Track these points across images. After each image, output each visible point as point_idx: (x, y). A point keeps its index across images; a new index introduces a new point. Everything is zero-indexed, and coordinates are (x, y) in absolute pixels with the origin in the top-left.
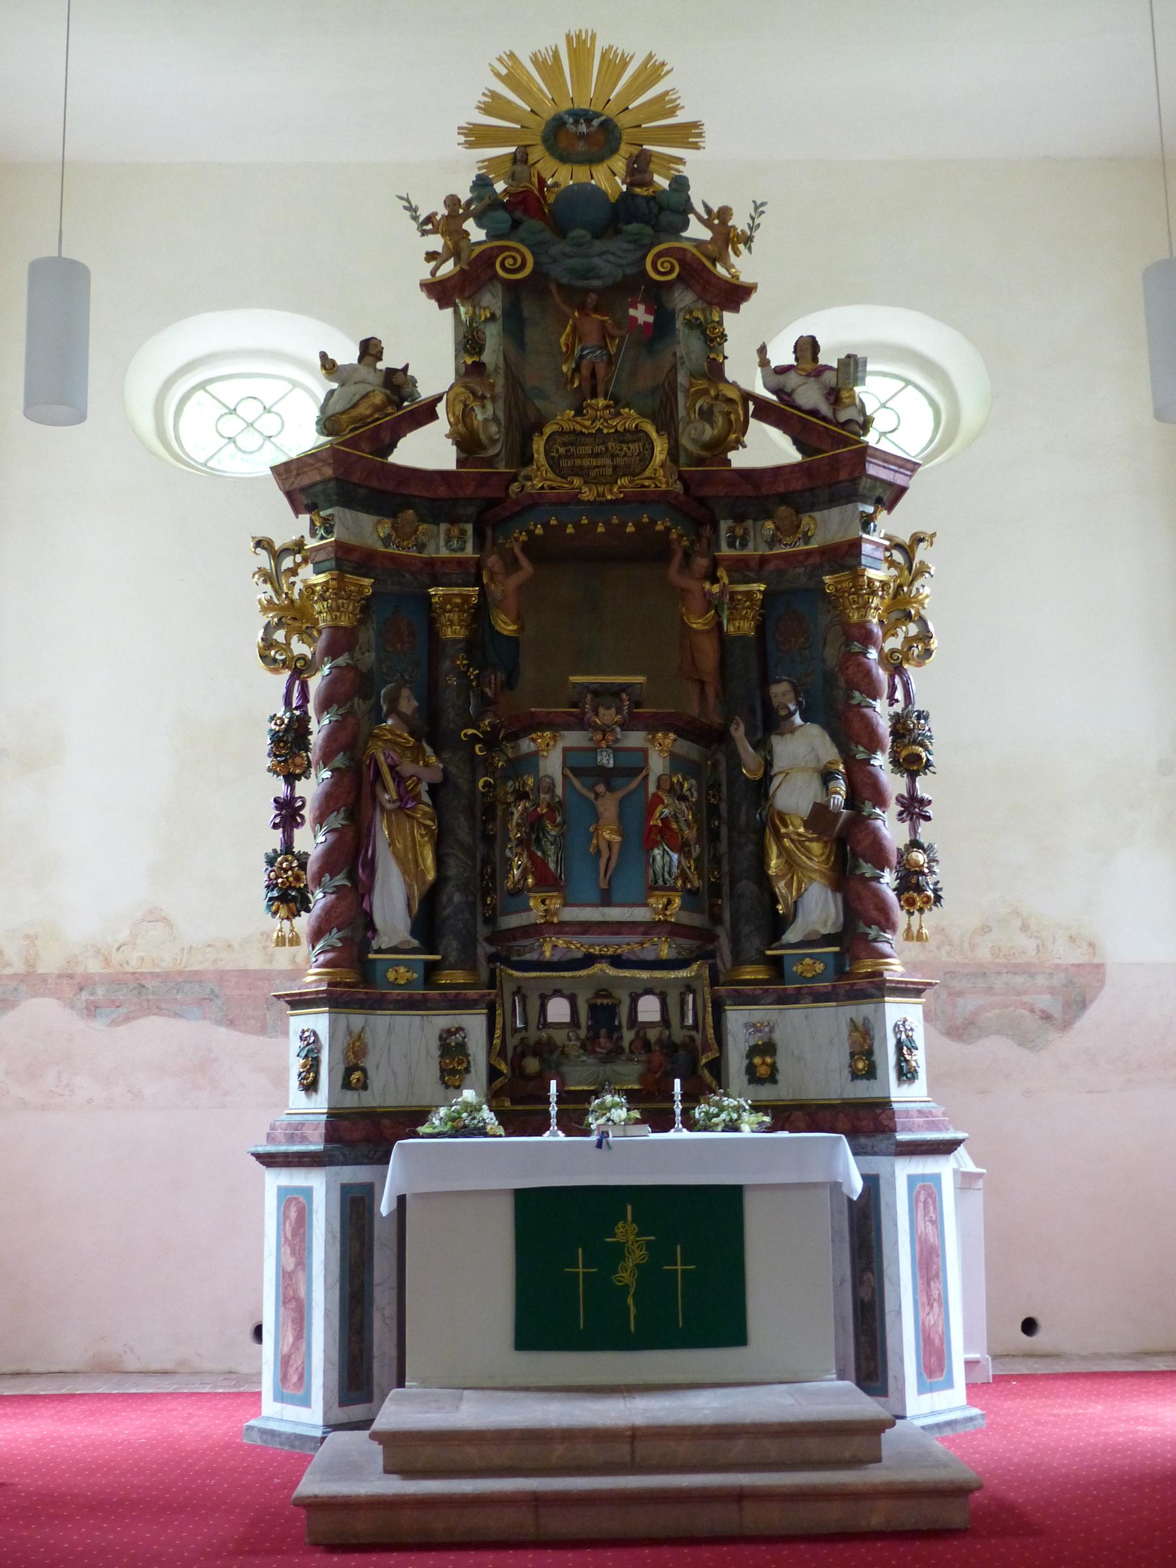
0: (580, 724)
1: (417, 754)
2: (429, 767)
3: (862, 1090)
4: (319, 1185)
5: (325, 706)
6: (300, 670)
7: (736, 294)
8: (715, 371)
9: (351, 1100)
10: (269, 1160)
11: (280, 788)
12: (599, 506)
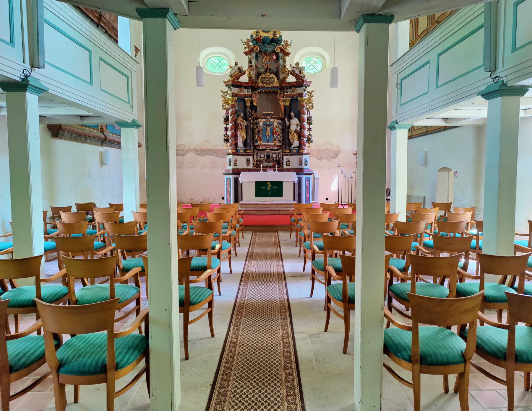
0: (265, 118)
1: (243, 121)
2: (245, 123)
3: (300, 167)
4: (232, 177)
5: (231, 115)
7: (288, 54)
8: (285, 67)
9: (235, 167)
10: (225, 174)
11: (225, 126)
12: (268, 88)
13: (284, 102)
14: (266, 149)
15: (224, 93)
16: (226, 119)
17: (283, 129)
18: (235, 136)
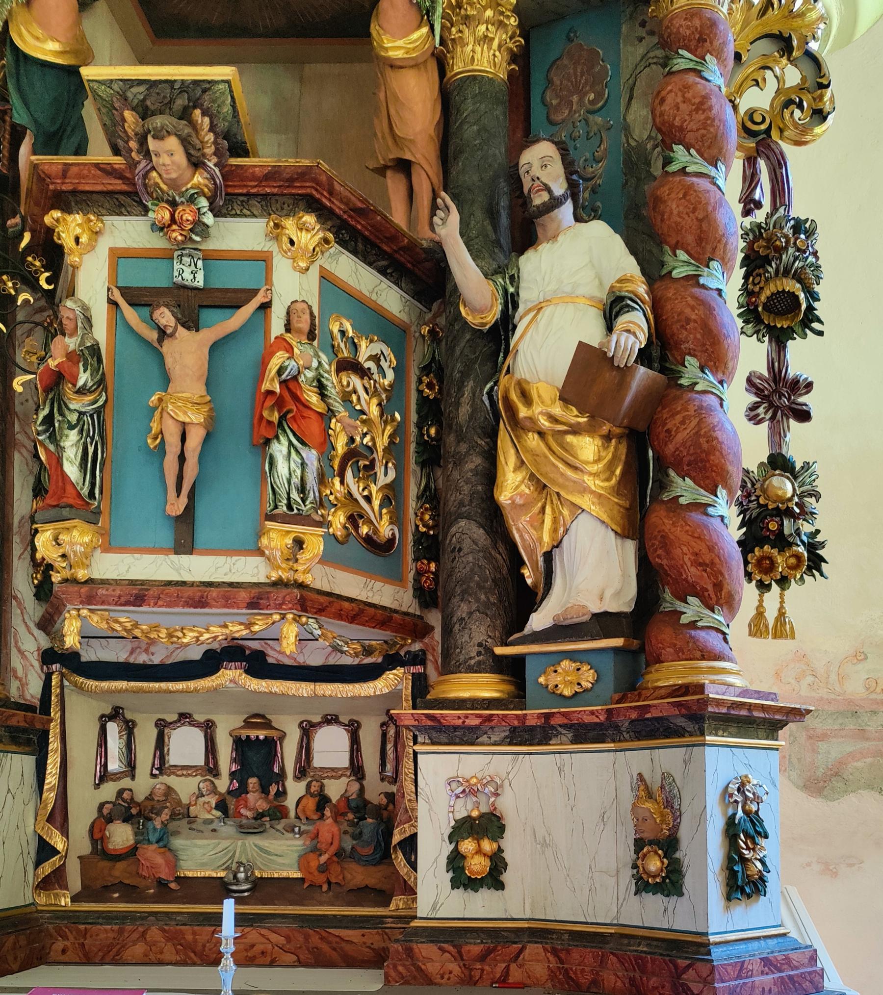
3: (652, 913)
14: (211, 662)
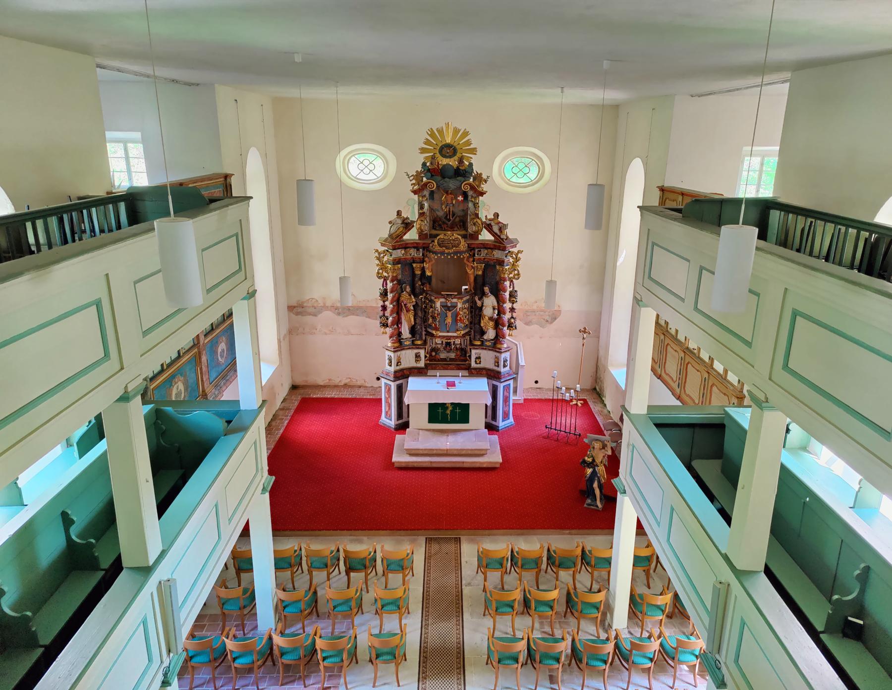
3: (496, 368)
6: (385, 279)
8: (477, 215)
9: (398, 368)
11: (381, 303)
12: (448, 254)
13: (474, 270)
15: (379, 254)
16: (384, 294)
17: (472, 307)
18: (398, 322)
